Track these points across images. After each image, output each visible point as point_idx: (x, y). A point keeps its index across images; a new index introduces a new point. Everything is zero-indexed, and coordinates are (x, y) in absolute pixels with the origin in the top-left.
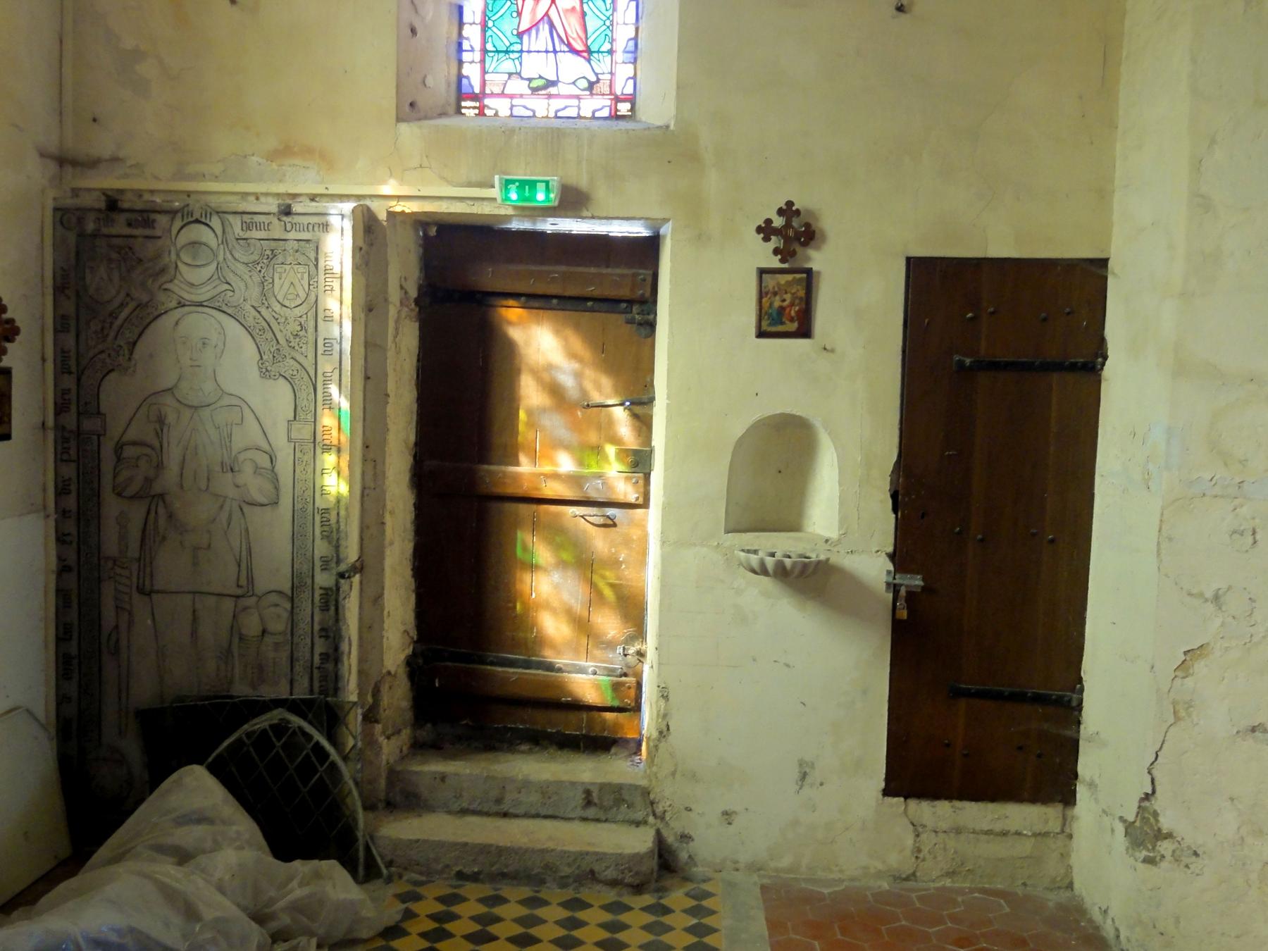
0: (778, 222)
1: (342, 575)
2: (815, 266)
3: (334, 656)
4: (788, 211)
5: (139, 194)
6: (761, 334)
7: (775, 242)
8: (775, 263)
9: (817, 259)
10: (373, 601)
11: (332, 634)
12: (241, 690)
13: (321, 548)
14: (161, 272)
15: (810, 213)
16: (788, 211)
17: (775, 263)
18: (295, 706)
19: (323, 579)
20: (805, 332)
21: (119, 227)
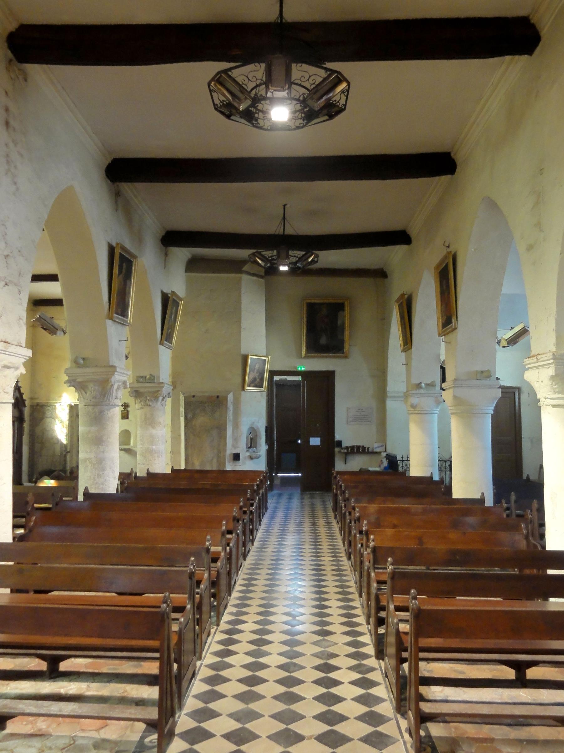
0: (124, 404)
1: (67, 453)
2: (129, 410)
3: (65, 464)
4: (125, 403)
5: (41, 402)
6: (122, 419)
7: (123, 407)
8: (123, 410)
9: (129, 409)
10: (72, 457)
11: (65, 461)
12: (53, 469)
13: (64, 449)
14: (44, 413)
15: (128, 403)
16: (125, 403)
17: (123, 410)
18: (60, 471)
19: (64, 453)
20: (128, 418)
21: (38, 408)
